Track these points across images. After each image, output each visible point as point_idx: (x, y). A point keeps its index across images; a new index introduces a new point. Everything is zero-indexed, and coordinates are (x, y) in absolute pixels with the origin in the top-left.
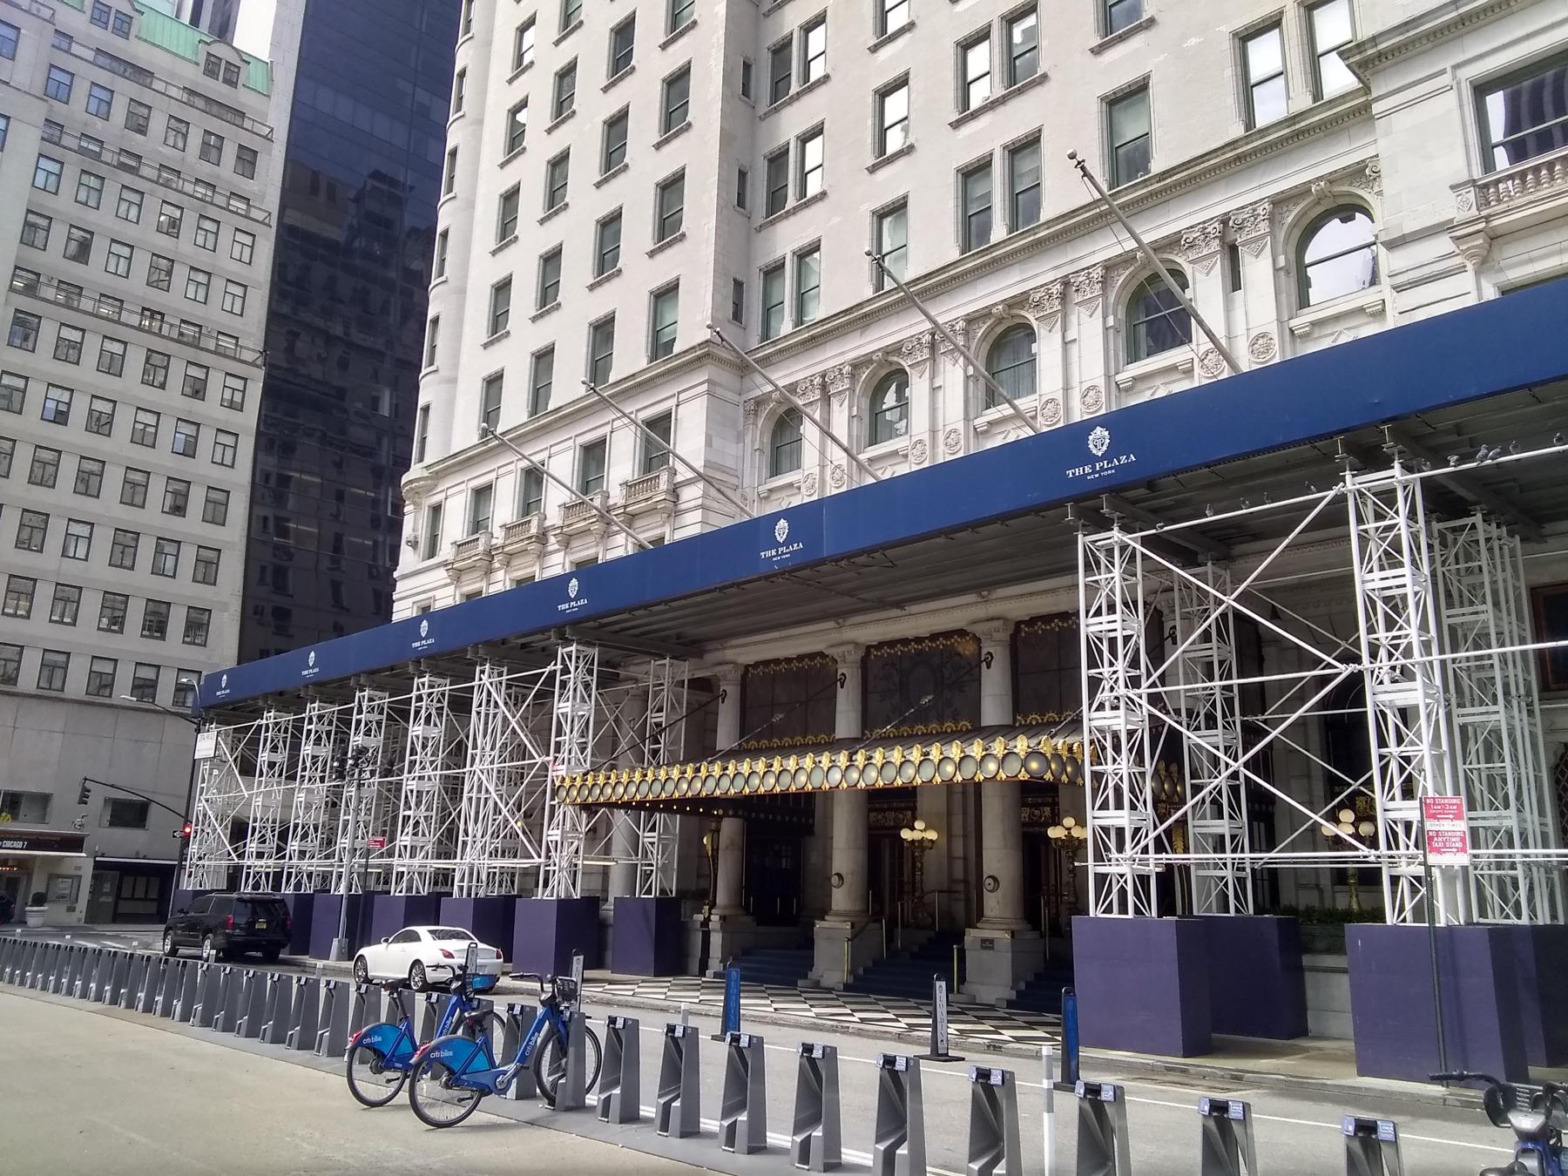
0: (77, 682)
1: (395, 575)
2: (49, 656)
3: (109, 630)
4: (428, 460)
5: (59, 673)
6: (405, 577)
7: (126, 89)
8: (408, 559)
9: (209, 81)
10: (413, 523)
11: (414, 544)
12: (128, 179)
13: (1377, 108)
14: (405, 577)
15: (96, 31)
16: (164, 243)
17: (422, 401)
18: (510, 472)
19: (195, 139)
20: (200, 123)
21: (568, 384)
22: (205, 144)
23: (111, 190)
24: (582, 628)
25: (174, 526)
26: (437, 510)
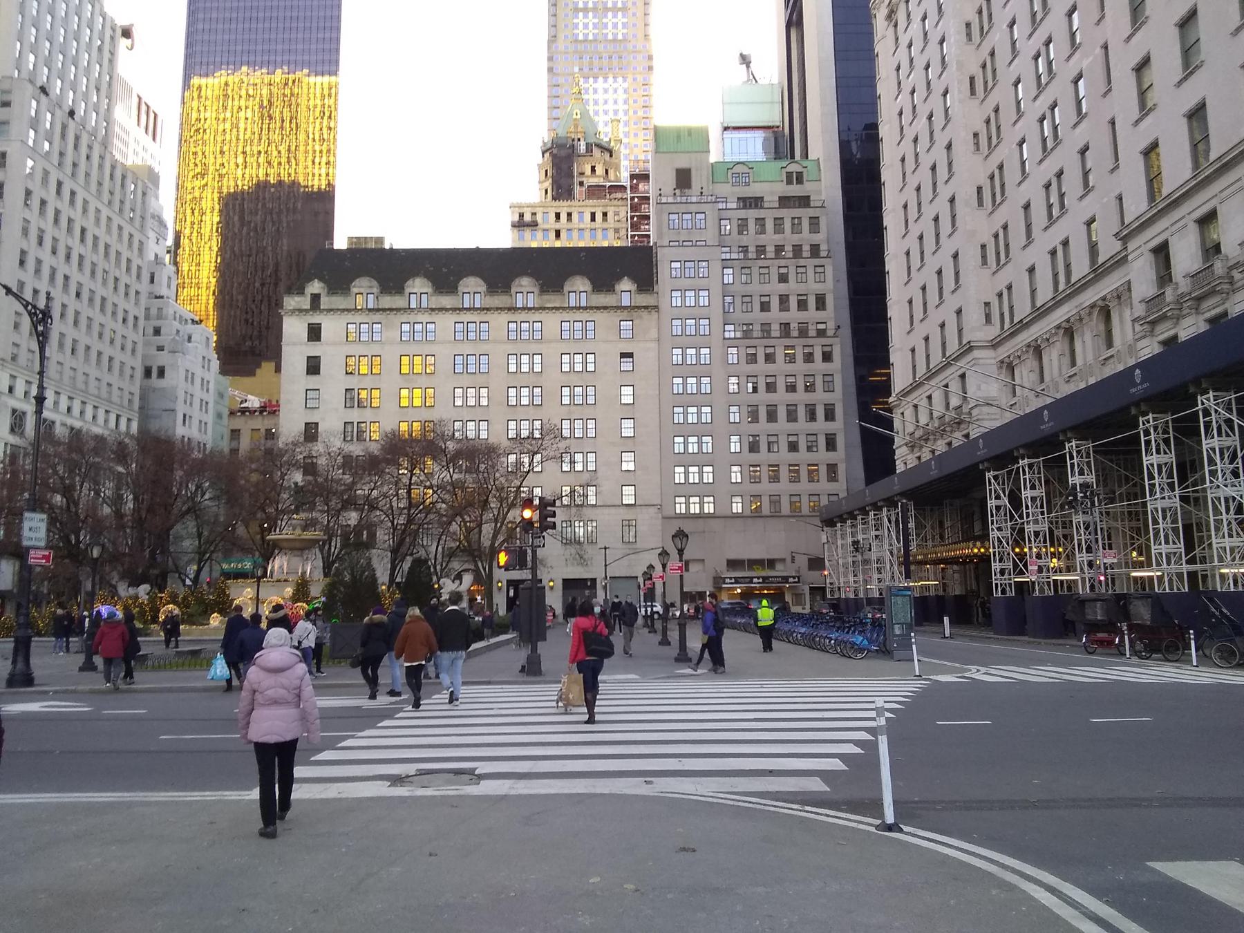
0: (785, 508)
1: (894, 447)
2: (772, 498)
3: (794, 482)
5: (777, 504)
6: (897, 448)
7: (752, 214)
9: (791, 187)
12: (761, 263)
13: (1130, 258)
14: (897, 448)
15: (737, 189)
16: (782, 288)
17: (891, 362)
18: (909, 408)
19: (788, 225)
20: (787, 214)
22: (793, 224)
23: (755, 271)
25: (813, 427)
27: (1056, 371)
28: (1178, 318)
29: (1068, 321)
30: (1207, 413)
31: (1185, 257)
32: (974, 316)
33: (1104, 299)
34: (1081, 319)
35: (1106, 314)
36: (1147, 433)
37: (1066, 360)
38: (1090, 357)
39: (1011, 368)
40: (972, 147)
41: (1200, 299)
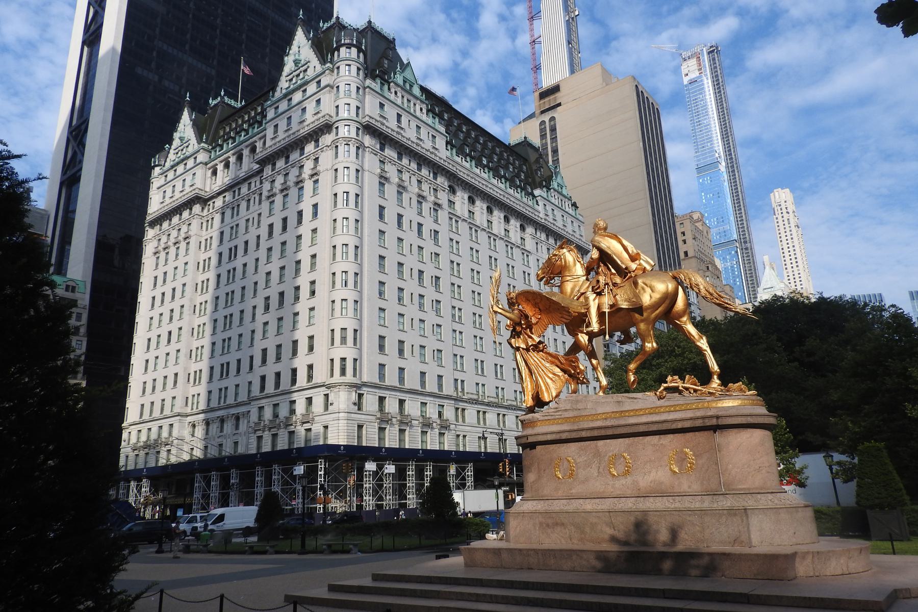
4: (128, 421)
8: (123, 443)
10: (125, 435)
11: (125, 441)
17: (127, 407)
21: (157, 413)
24: (147, 477)
26: (130, 433)
27: (214, 433)
28: (264, 431)
29: (223, 416)
30: (275, 470)
31: (268, 414)
32: (179, 402)
33: (238, 413)
34: (228, 417)
35: (238, 419)
36: (258, 471)
37: (219, 429)
38: (229, 432)
39: (194, 426)
40: (191, 334)
41: (271, 428)
